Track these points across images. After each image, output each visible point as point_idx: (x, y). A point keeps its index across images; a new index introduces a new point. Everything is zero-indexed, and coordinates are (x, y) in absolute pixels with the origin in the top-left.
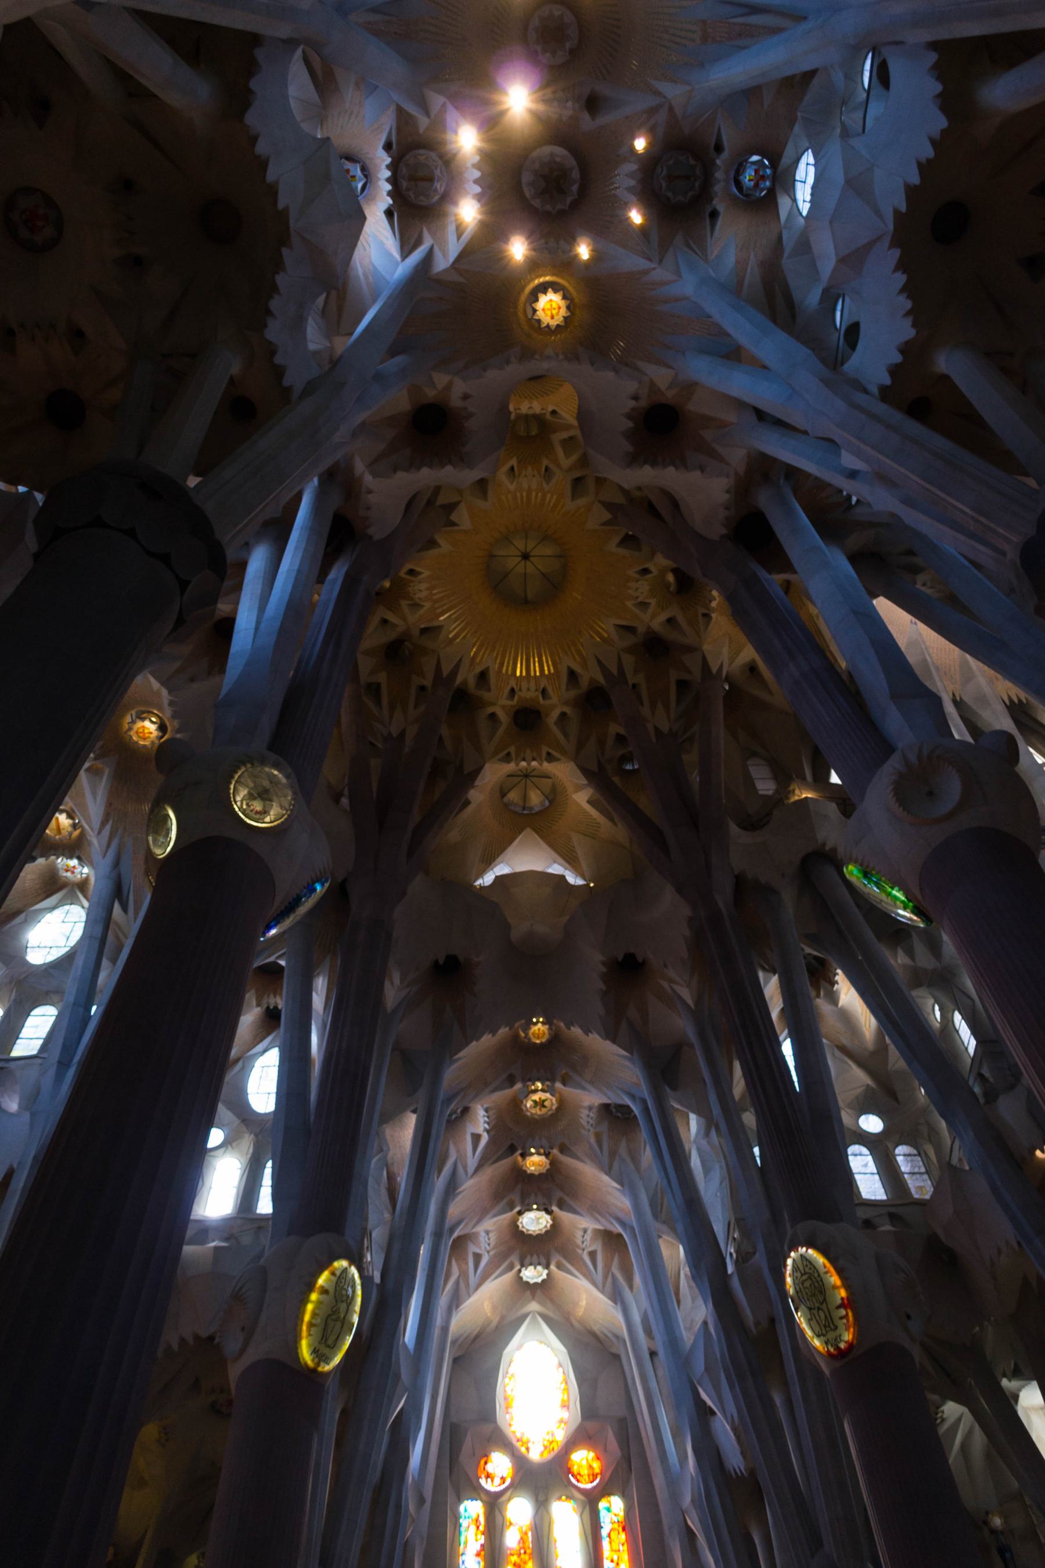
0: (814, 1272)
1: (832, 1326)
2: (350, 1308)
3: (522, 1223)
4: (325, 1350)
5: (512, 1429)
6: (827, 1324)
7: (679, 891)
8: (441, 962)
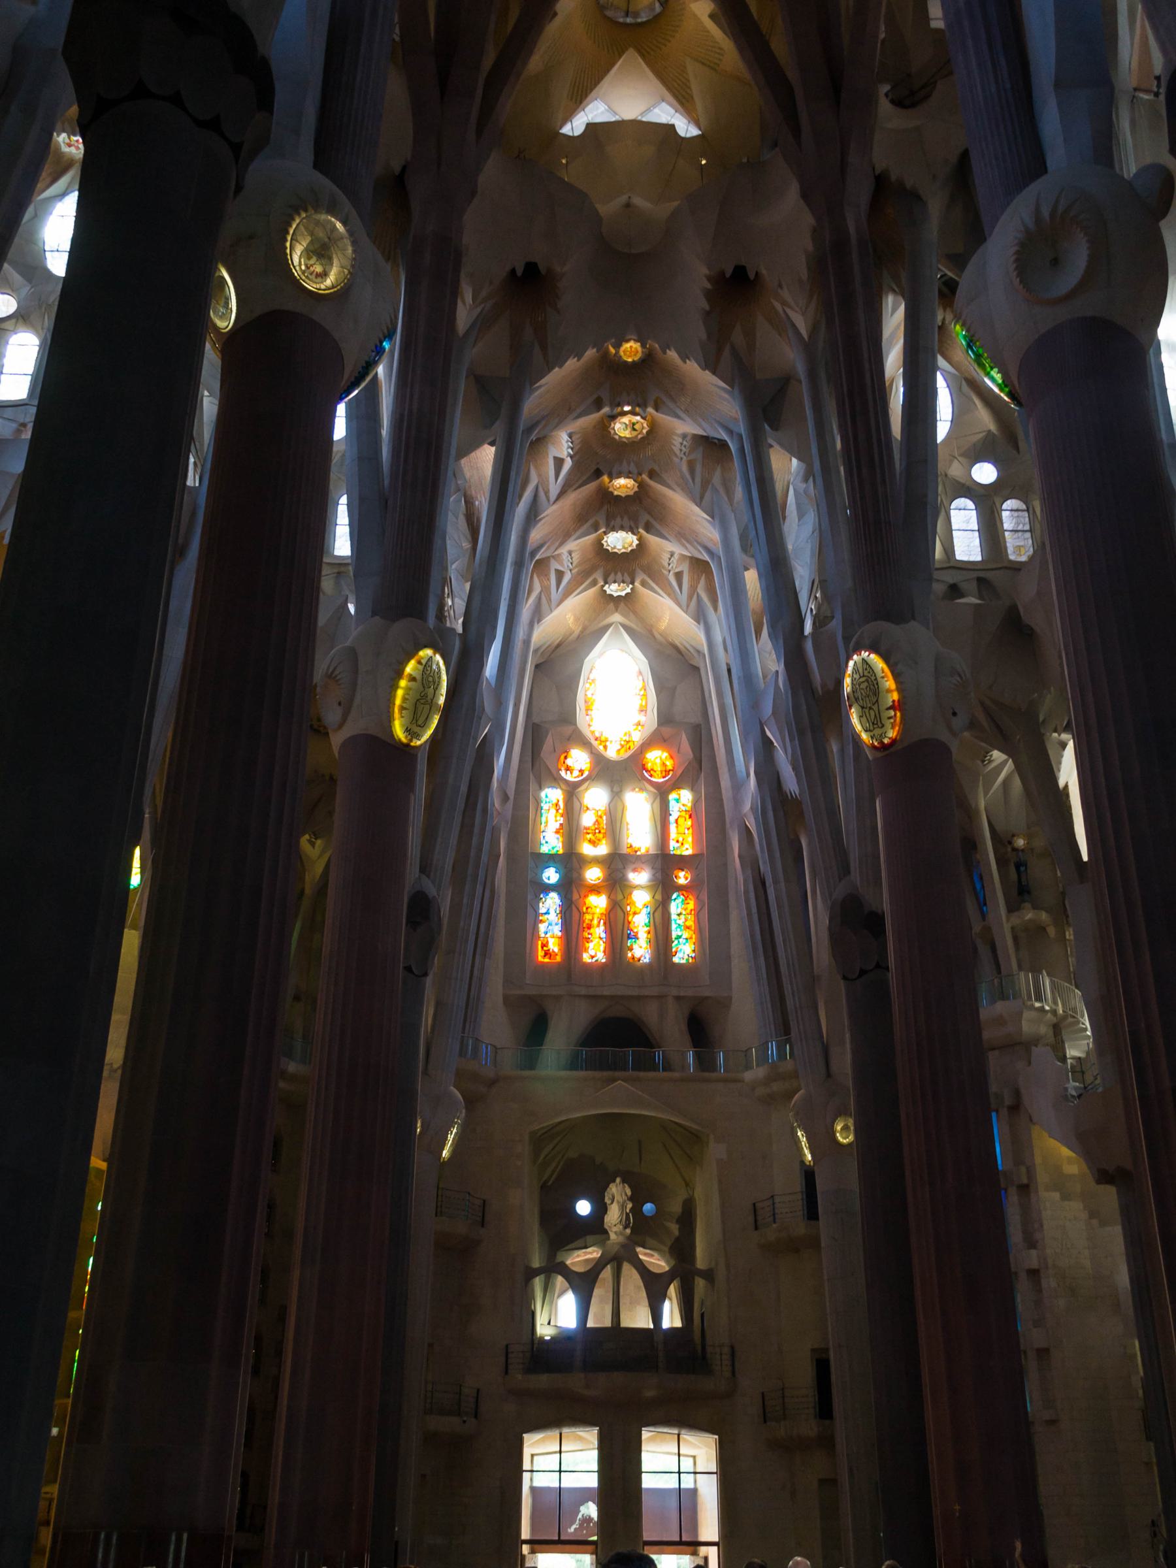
0: (872, 676)
1: (879, 723)
2: (437, 692)
3: (607, 542)
4: (416, 729)
5: (592, 728)
6: (875, 722)
7: (805, 196)
8: (519, 272)
